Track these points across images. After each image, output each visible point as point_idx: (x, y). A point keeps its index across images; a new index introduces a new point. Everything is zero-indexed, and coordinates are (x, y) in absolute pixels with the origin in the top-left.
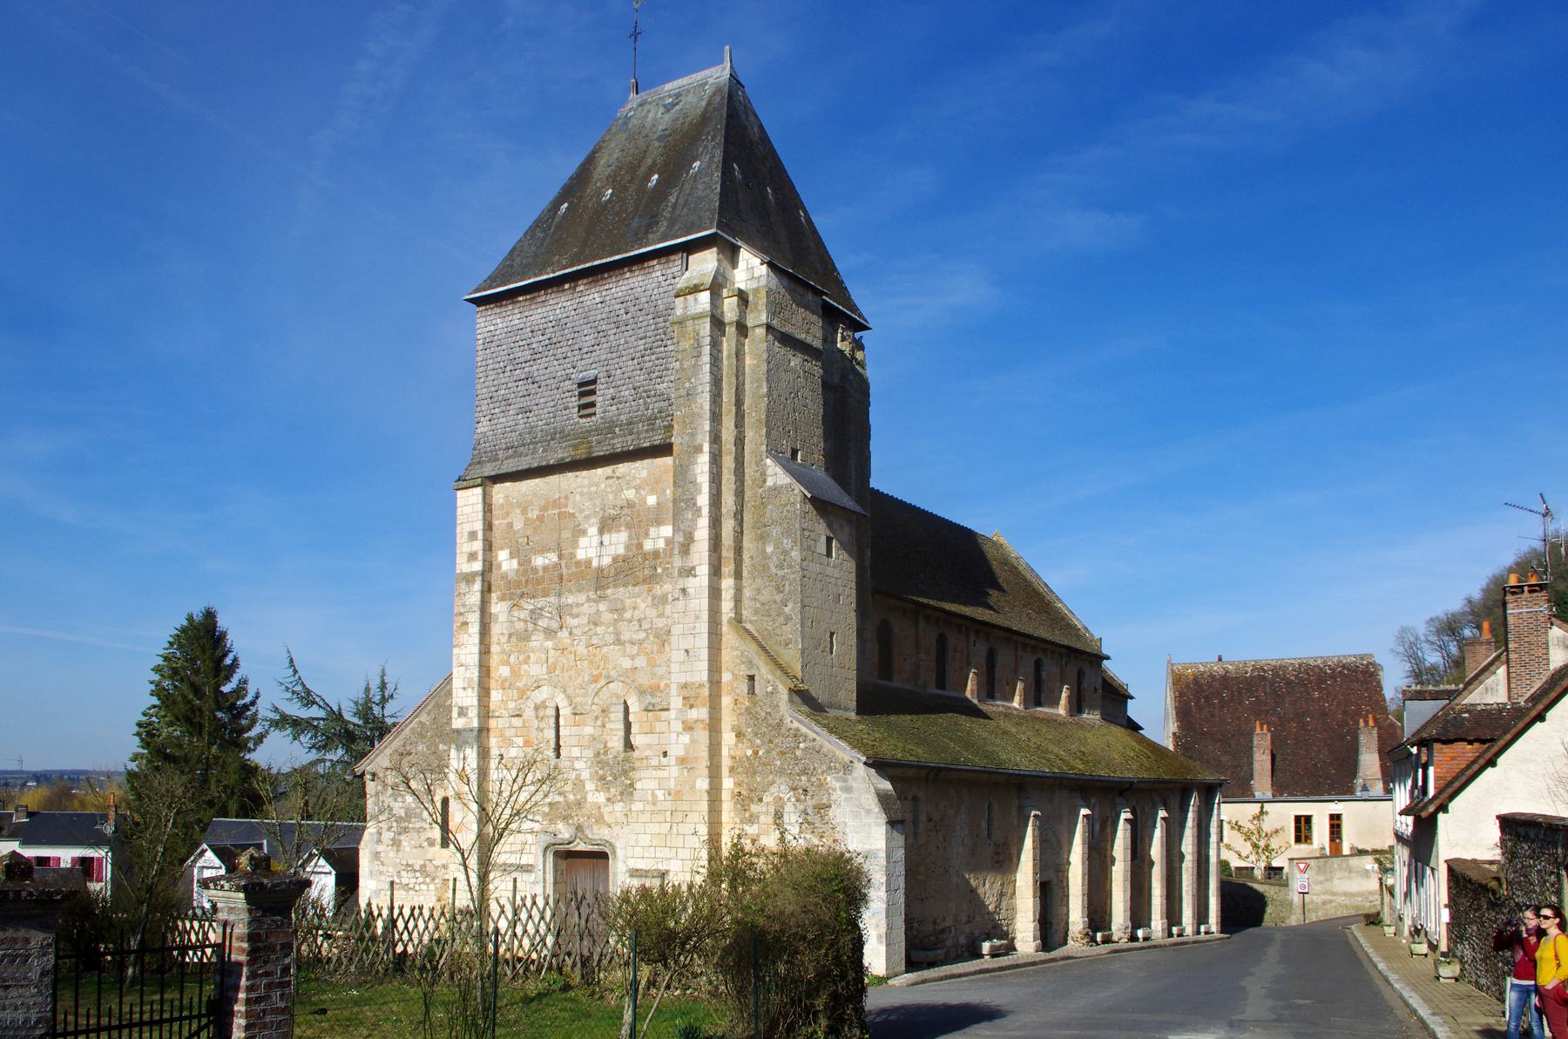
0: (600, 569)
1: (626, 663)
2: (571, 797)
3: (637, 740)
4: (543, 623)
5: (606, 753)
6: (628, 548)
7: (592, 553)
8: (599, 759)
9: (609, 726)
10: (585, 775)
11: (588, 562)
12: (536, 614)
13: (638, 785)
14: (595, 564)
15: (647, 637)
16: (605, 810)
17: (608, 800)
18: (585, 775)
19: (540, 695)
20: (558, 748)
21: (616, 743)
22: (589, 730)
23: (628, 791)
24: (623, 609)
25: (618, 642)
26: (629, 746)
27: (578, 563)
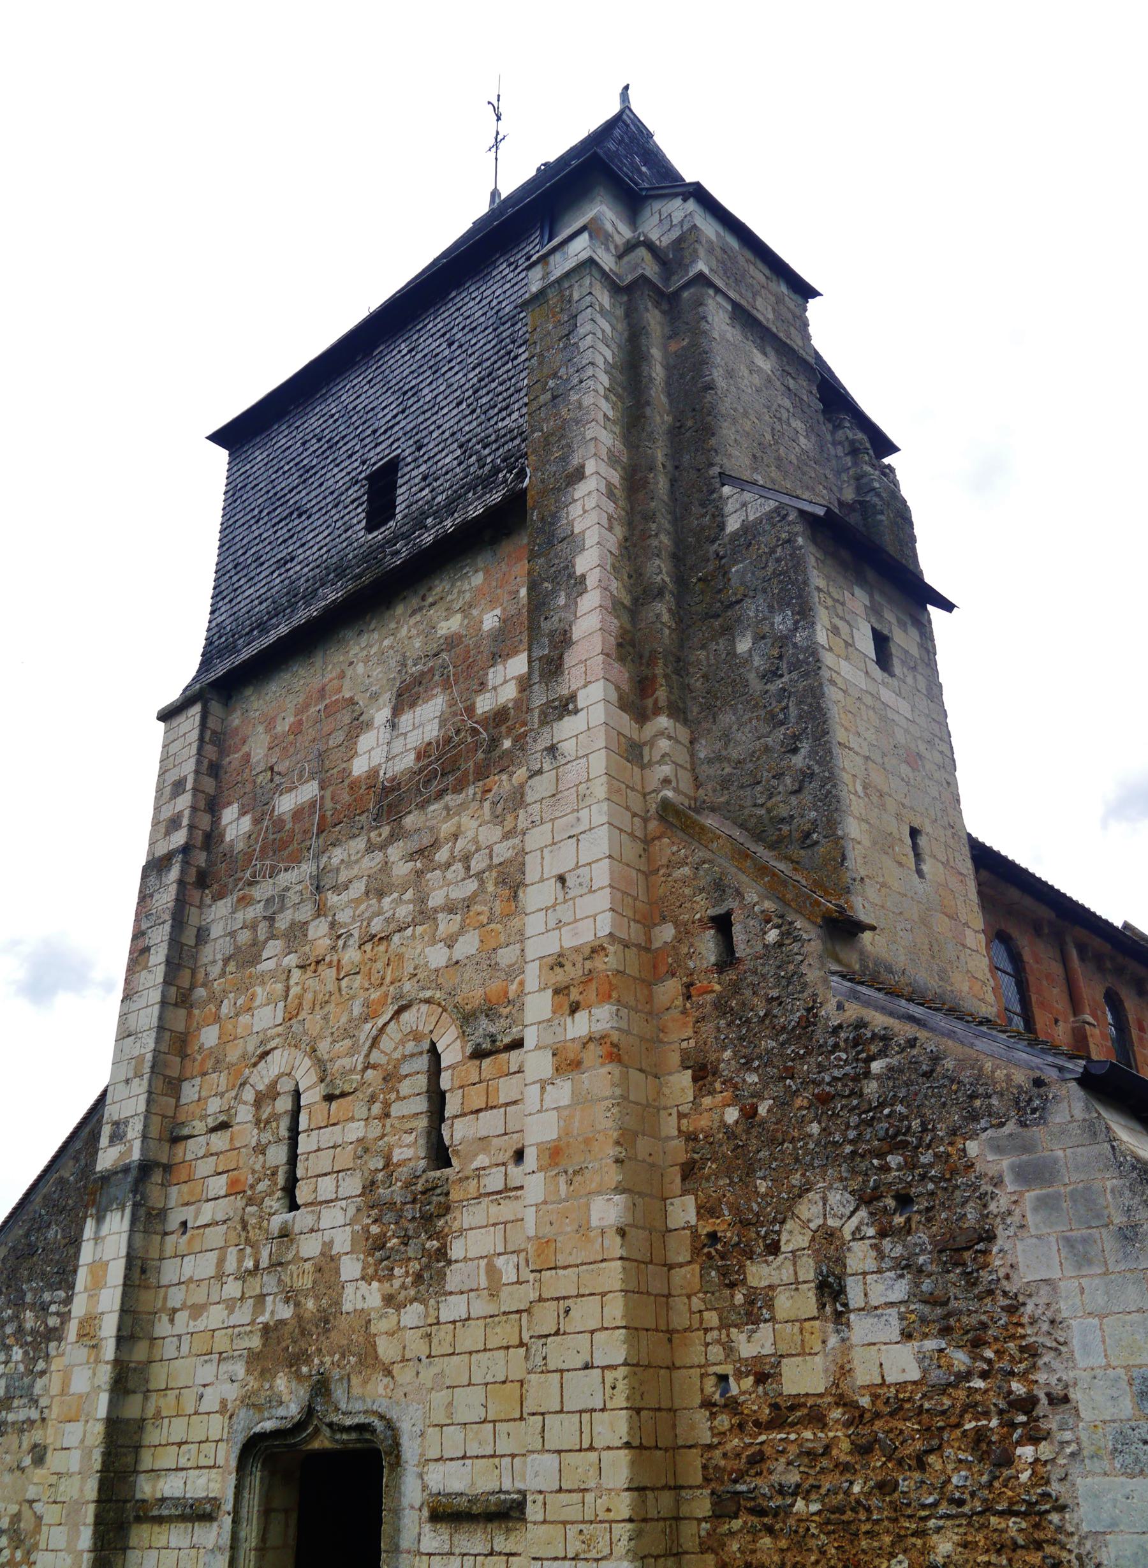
2: (310, 1304)
3: (457, 1132)
9: (396, 1110)
10: (342, 1241)
13: (456, 1250)
16: (380, 1326)
17: (389, 1300)
21: (409, 1150)
22: (355, 1131)
26: (440, 1155)
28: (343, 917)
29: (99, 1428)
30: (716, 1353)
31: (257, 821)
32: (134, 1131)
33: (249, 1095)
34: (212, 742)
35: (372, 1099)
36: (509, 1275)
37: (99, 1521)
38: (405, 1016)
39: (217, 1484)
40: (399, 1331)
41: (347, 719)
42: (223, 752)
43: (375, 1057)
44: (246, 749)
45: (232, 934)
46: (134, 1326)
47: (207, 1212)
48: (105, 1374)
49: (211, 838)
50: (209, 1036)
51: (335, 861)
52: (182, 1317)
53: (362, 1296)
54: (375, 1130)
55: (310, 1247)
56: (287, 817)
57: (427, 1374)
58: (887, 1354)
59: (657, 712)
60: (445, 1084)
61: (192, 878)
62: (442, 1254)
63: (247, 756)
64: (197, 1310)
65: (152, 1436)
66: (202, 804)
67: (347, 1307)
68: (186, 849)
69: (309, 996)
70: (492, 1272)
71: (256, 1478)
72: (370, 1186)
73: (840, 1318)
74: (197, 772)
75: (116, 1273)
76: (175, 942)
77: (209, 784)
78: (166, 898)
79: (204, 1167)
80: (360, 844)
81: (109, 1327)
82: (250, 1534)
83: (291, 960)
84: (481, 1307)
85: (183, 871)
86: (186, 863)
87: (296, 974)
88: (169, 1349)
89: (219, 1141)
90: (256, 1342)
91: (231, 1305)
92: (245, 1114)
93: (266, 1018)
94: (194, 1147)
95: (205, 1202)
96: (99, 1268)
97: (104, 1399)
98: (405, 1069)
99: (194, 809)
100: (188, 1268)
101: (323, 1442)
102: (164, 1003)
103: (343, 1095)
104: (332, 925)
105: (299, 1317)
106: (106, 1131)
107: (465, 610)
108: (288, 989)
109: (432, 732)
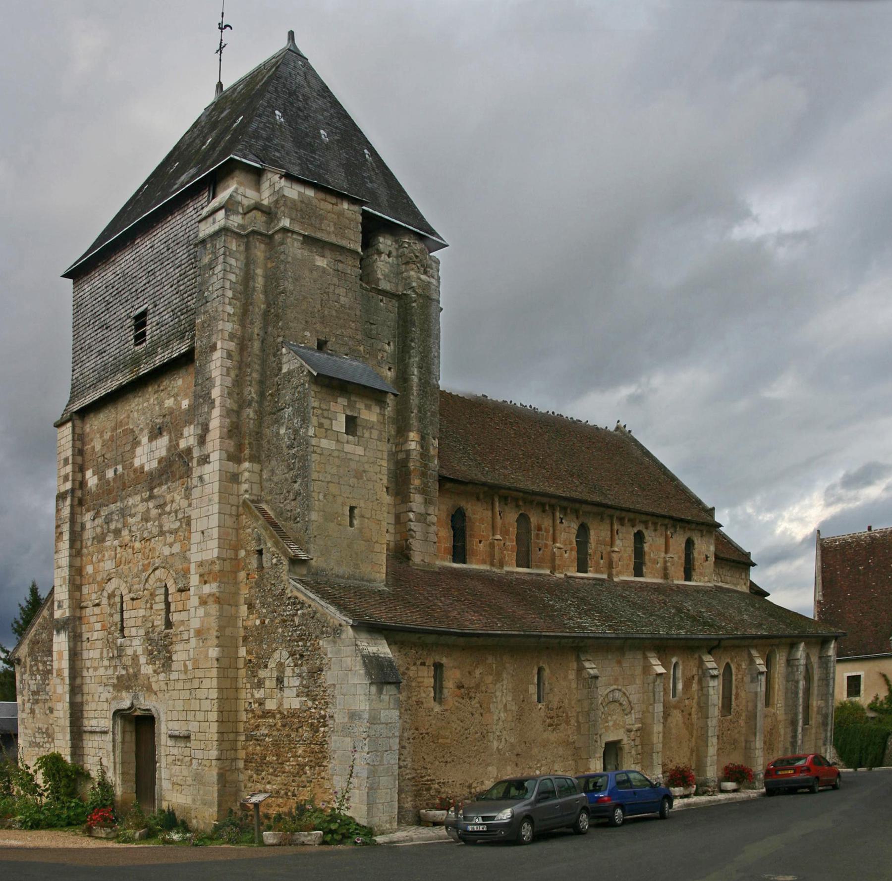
0: (151, 473)
1: (167, 551)
2: (131, 670)
3: (175, 617)
4: (113, 526)
5: (153, 632)
6: (169, 450)
7: (144, 460)
8: (148, 639)
9: (155, 607)
10: (140, 651)
11: (142, 467)
12: (108, 521)
13: (174, 658)
14: (146, 469)
15: (181, 526)
17: (155, 671)
18: (140, 651)
19: (110, 587)
20: (122, 629)
21: (159, 622)
22: (142, 612)
23: (167, 664)
24: (165, 504)
26: (169, 624)
27: (135, 471)
28: (133, 529)
29: (68, 705)
30: (249, 696)
31: (99, 479)
32: (66, 604)
33: (105, 594)
34: (79, 440)
35: (147, 602)
36: (190, 668)
37: (72, 732)
38: (157, 572)
39: (106, 723)
40: (158, 681)
41: (131, 439)
42: (84, 444)
43: (147, 586)
44: (92, 444)
45: (94, 528)
46: (75, 672)
47: (96, 636)
48: (67, 688)
49: (83, 484)
50: (89, 569)
51: (130, 503)
52: (91, 670)
53: (147, 669)
54: (148, 613)
55: (129, 651)
56: (111, 480)
57: (167, 696)
58: (292, 701)
59: (245, 460)
60: (170, 600)
61: (76, 502)
62: (170, 658)
63: (93, 448)
64: (96, 669)
65: (86, 708)
66: (77, 470)
67: (142, 672)
68: (73, 490)
69: (124, 559)
70: (185, 666)
71: (119, 722)
72: (147, 633)
73: (281, 689)
74: (73, 455)
75: (66, 655)
76: (72, 532)
77: (79, 459)
78: (66, 512)
79: (93, 619)
80: (138, 498)
81: (66, 673)
82: (119, 738)
83: (116, 543)
84: (182, 677)
85: (72, 500)
86: (73, 497)
87: (119, 548)
88: (88, 680)
89: (97, 610)
90: (115, 681)
91: (106, 668)
92: (105, 601)
93: (109, 565)
94: (88, 612)
95: (94, 633)
96: (60, 653)
97: (68, 696)
98: (157, 593)
99: (73, 472)
100: (91, 654)
101: (138, 713)
102: (70, 556)
103: (137, 599)
104: (130, 531)
105: (128, 674)
106: (56, 604)
107: (176, 396)
108: (116, 554)
109: (164, 453)
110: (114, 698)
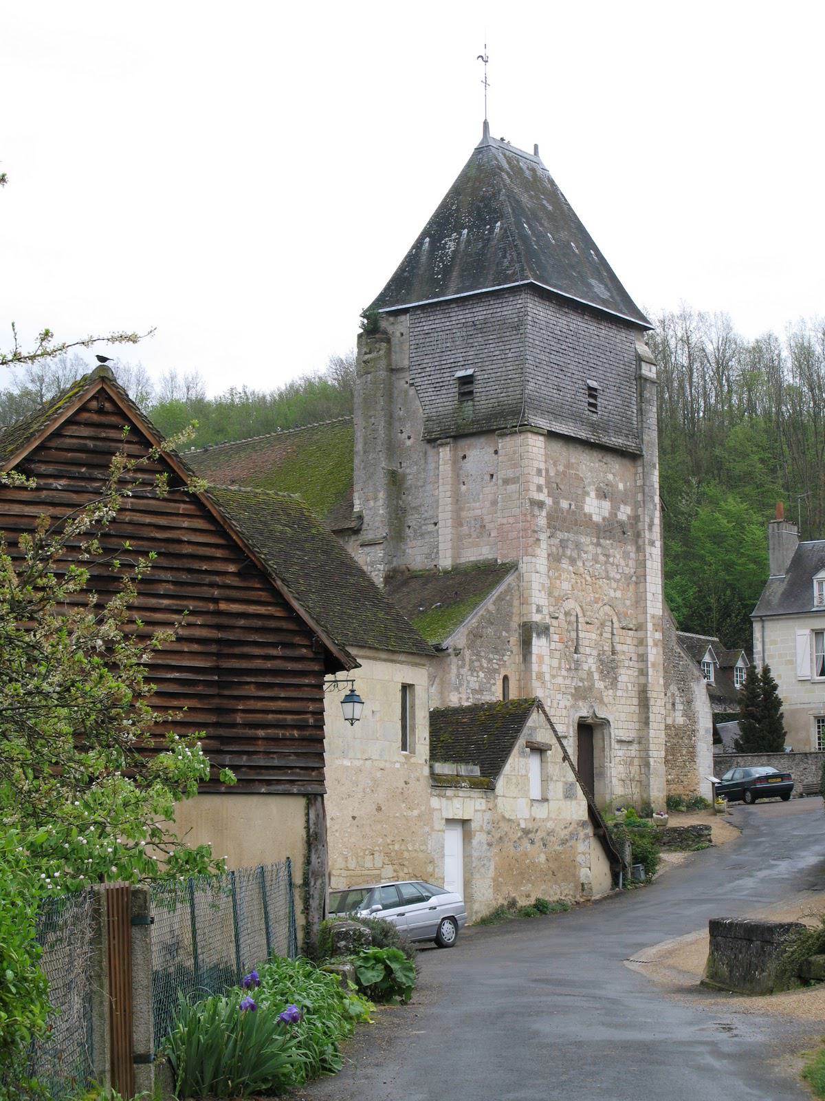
9: (605, 635)
10: (594, 668)
17: (605, 687)
18: (594, 668)
21: (607, 648)
23: (614, 681)
25: (608, 578)
36: (630, 689)
53: (599, 685)
55: (585, 667)
90: (573, 691)
110: (572, 706)
